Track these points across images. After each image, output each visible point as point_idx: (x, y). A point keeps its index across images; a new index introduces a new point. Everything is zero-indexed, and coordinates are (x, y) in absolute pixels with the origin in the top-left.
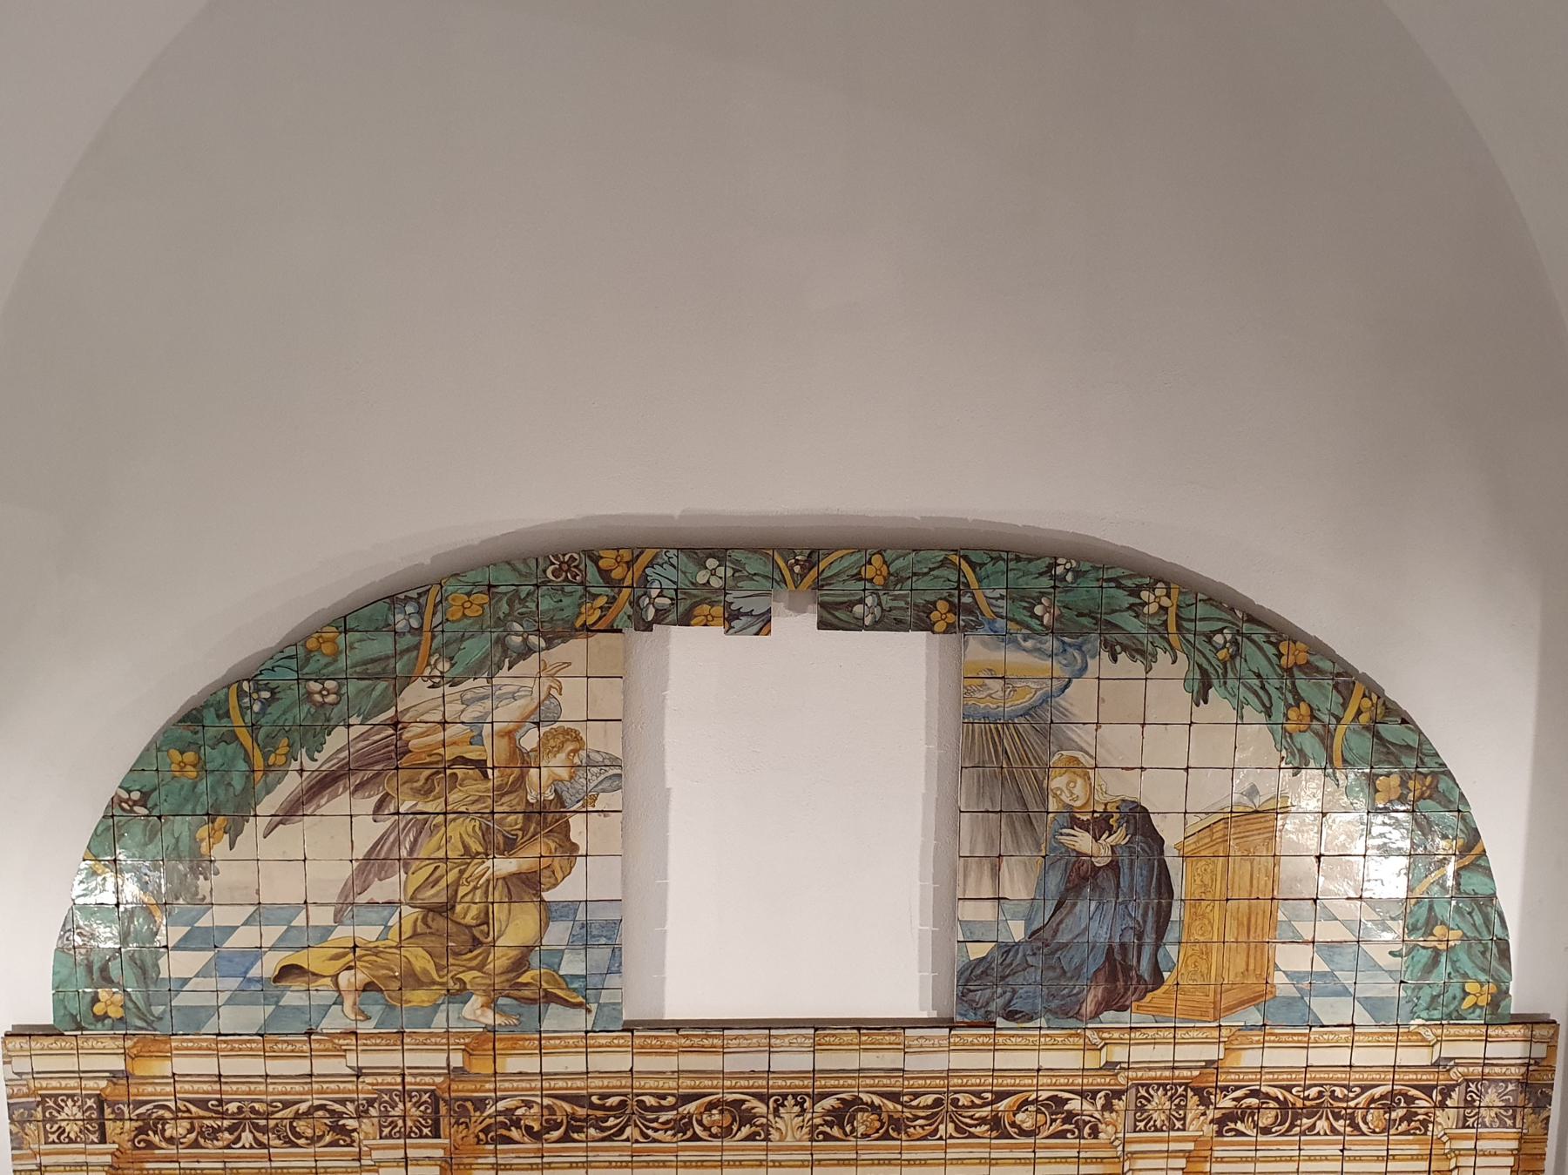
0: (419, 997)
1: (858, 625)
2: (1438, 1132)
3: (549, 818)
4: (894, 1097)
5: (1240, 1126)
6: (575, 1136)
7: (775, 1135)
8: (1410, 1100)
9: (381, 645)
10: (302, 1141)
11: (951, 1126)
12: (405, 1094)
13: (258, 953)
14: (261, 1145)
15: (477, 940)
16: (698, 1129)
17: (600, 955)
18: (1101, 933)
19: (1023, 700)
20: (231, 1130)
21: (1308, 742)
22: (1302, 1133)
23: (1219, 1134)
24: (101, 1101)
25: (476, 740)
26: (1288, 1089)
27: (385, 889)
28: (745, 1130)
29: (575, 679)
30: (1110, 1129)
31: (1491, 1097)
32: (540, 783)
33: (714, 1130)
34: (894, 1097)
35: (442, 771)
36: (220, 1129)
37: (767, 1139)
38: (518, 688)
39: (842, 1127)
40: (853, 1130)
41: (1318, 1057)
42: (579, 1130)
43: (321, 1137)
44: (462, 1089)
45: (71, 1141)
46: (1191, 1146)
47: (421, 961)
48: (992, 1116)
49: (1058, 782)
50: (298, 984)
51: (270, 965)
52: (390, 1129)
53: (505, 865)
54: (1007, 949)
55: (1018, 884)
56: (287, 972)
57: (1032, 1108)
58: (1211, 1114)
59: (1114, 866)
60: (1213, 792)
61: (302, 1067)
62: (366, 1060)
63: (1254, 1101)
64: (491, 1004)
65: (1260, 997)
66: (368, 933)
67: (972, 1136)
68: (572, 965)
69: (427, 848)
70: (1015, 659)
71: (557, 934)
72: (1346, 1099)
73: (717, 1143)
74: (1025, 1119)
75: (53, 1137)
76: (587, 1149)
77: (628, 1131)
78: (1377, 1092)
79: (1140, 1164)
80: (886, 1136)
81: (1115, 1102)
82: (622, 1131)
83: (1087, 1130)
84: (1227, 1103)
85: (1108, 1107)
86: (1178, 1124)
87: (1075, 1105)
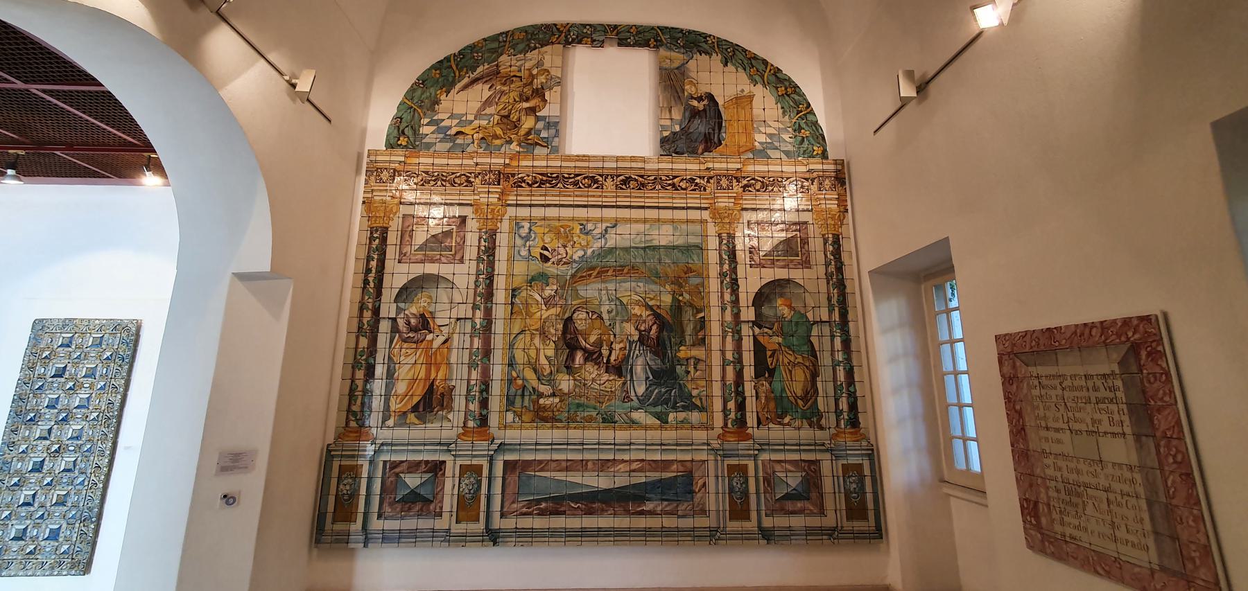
0: (497, 142)
1: (628, 45)
3: (539, 93)
4: (642, 176)
9: (495, 45)
12: (491, 171)
13: (450, 128)
15: (516, 126)
17: (553, 131)
18: (702, 129)
19: (676, 64)
21: (757, 78)
24: (395, 170)
25: (520, 71)
27: (490, 110)
29: (550, 56)
31: (827, 182)
32: (537, 83)
34: (642, 176)
35: (508, 80)
38: (533, 55)
41: (771, 168)
44: (508, 170)
47: (499, 132)
48: (671, 183)
49: (687, 87)
50: (461, 137)
51: (453, 131)
52: (484, 182)
53: (526, 105)
54: (674, 133)
55: (677, 114)
56: (458, 133)
59: (704, 110)
60: (731, 91)
61: (459, 162)
62: (479, 160)
64: (519, 145)
65: (752, 150)
66: (484, 123)
68: (544, 134)
69: (504, 99)
70: (674, 54)
71: (540, 125)
74: (683, 185)
84: (745, 182)
87: (698, 181)
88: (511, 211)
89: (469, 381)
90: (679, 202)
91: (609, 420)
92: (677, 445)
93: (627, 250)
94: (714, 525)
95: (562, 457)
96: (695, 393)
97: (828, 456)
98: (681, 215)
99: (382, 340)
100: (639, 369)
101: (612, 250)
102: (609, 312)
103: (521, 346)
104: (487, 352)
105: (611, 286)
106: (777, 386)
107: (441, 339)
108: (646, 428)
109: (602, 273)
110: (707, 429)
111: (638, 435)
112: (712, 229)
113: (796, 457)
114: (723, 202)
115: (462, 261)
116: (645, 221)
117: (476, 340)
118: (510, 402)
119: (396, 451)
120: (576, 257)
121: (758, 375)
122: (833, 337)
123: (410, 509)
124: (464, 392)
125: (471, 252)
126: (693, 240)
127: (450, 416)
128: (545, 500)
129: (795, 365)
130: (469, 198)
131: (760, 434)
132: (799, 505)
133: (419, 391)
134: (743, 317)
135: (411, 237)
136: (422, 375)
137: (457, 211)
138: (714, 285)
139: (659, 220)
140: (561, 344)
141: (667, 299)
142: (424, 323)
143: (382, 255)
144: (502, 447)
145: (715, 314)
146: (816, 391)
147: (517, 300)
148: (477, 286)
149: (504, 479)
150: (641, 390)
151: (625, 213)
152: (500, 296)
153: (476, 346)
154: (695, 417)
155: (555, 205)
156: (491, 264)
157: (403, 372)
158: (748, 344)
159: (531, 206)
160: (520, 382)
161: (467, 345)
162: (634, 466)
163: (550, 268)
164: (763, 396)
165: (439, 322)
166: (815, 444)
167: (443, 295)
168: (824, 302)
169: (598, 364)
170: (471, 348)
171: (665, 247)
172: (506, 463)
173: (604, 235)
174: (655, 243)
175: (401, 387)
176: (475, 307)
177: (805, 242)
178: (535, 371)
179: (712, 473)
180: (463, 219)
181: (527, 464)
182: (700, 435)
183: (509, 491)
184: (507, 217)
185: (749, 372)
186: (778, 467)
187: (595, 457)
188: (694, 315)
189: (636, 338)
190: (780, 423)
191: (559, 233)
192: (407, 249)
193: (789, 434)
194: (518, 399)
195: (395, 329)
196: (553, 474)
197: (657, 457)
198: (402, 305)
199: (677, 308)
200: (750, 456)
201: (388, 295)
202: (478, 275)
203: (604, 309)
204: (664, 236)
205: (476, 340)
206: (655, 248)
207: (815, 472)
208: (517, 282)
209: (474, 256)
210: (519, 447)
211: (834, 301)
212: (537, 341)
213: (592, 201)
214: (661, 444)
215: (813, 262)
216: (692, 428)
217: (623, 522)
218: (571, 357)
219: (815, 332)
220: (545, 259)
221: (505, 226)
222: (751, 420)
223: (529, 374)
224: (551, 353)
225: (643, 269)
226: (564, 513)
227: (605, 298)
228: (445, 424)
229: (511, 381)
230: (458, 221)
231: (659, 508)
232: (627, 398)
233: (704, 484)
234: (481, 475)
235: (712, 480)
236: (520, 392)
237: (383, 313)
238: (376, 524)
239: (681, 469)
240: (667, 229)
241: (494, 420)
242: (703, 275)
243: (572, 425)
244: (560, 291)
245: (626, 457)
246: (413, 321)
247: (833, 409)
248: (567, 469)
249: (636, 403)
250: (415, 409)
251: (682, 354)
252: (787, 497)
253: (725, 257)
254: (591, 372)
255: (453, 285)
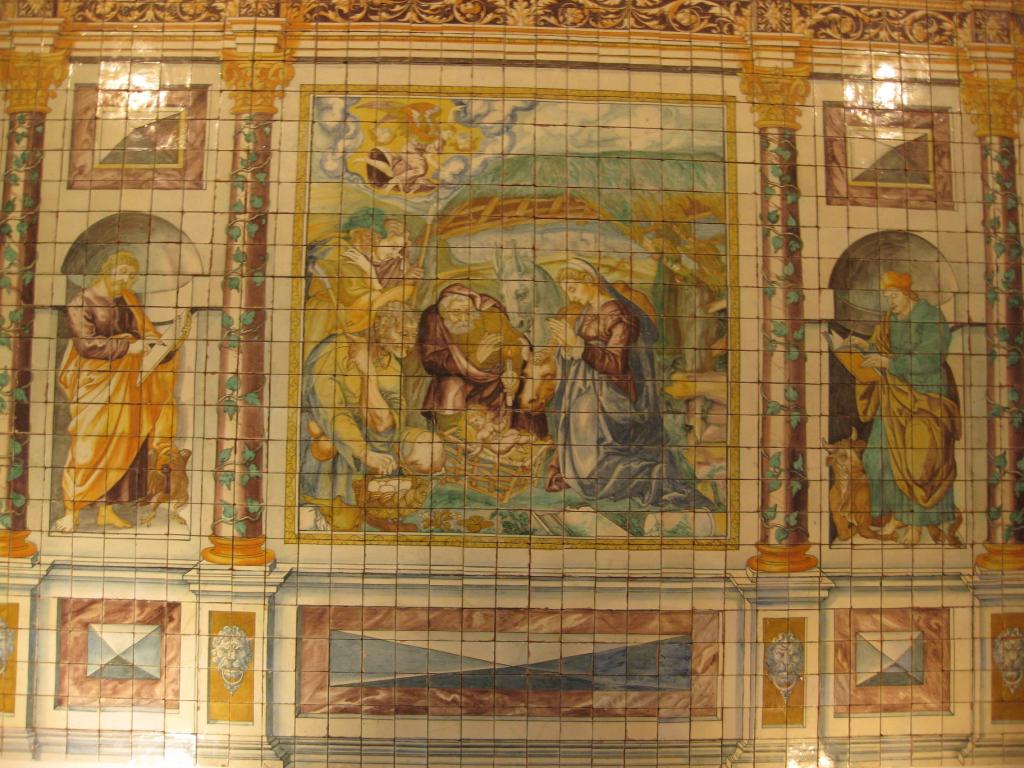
2: (960, 44)
5: (829, 31)
6: (372, 17)
7: (510, 21)
8: (940, 22)
10: (186, 18)
11: (632, 20)
14: (158, 19)
16: (457, 15)
20: (140, 9)
22: (871, 39)
23: (816, 36)
26: (858, 8)
28: (490, 17)
30: (741, 28)
33: (468, 16)
36: (132, 9)
37: (505, 24)
39: (556, 16)
40: (565, 20)
42: (375, 13)
43: (199, 15)
45: (34, 16)
46: (796, 44)
57: (687, 11)
58: (809, 22)
63: (835, 16)
67: (647, 28)
72: (897, 18)
73: (469, 25)
74: (684, 18)
75: (23, 12)
76: (380, 27)
77: (409, 16)
78: (918, 14)
79: (764, 54)
80: (587, 25)
81: (743, 10)
82: (404, 15)
83: (725, 28)
84: (818, 16)
85: (738, 13)
86: (787, 28)
87: (716, 10)
88: (304, 74)
89: (219, 440)
90: (674, 57)
91: (518, 529)
92: (662, 579)
93: (559, 159)
94: (731, 733)
95: (418, 601)
96: (702, 472)
97: (965, 599)
98: (678, 84)
99: (41, 354)
100: (583, 421)
101: (525, 160)
102: (519, 296)
103: (329, 368)
104: (256, 381)
105: (524, 240)
106: (873, 458)
107: (159, 353)
108: (597, 544)
109: (503, 212)
110: (726, 547)
111: (579, 559)
112: (746, 118)
113: (902, 601)
114: (770, 60)
115: (198, 184)
116: (599, 96)
117: (232, 355)
118: (306, 489)
119: (80, 580)
120: (446, 174)
121: (836, 437)
122: (991, 355)
123: (115, 691)
124: (211, 464)
125: (218, 165)
126: (705, 142)
127: (184, 513)
128: (386, 685)
129: (912, 415)
130: (213, 46)
131: (834, 557)
132: (902, 694)
133: (119, 462)
134: (809, 312)
135: (92, 131)
136: (124, 426)
137: (188, 76)
138: (748, 240)
139: (628, 95)
140: (414, 365)
141: (646, 269)
142: (124, 318)
143: (36, 168)
144: (293, 579)
145: (749, 303)
146: (953, 468)
147: (318, 270)
148: (231, 239)
149: (297, 640)
150: (587, 464)
151: (555, 79)
152: (281, 260)
153: (232, 367)
154: (703, 523)
155: (401, 60)
156: (262, 191)
157: (86, 421)
158: (817, 369)
159: (346, 61)
160: (327, 445)
161: (214, 366)
162: (571, 621)
163: (389, 199)
164: (844, 478)
165: (154, 315)
166: (944, 576)
167: (160, 258)
168: (978, 280)
169: (495, 408)
170: (222, 373)
171: (646, 157)
172: (303, 611)
173: (507, 126)
174: (622, 145)
175: (84, 451)
176: (228, 284)
177: (942, 151)
178: (359, 421)
179: (732, 635)
180: (201, 93)
181: (346, 615)
182: (711, 560)
183: (314, 662)
184: (294, 85)
185: (817, 430)
186: (865, 623)
187: (489, 603)
188: (705, 306)
189: (578, 353)
190: (875, 535)
191: (409, 121)
192: (84, 159)
193: (895, 557)
194: (324, 483)
195: (65, 331)
196: (402, 635)
197: (619, 604)
198: (77, 279)
199: (670, 288)
200: (809, 601)
201: (50, 257)
202: (233, 214)
203: (509, 291)
204: (640, 130)
205: (232, 355)
206: (619, 156)
207: (938, 630)
208: (320, 228)
209: (225, 172)
210: (328, 579)
211: (999, 279)
212: (362, 357)
213: (482, 50)
214: (629, 579)
215: (957, 195)
216: (695, 544)
217: (544, 729)
218: (437, 393)
219: (957, 343)
220: (380, 179)
221: (290, 105)
222: (817, 529)
223: (347, 430)
224: (392, 383)
225: (592, 200)
226: (425, 710)
227: (509, 265)
228: (175, 528)
229: (308, 443)
230: (191, 96)
231: (620, 704)
232: (556, 483)
233: (715, 658)
234: (251, 633)
235: (731, 649)
236: (327, 466)
237: (39, 298)
238: (51, 718)
239: (668, 627)
240: (648, 115)
241: (274, 524)
242: (722, 213)
243: (439, 536)
244: (412, 250)
245: (555, 604)
246: (101, 314)
247: (982, 505)
248: (429, 626)
249: (575, 493)
250: (113, 495)
251: (676, 390)
252: (882, 680)
253: (773, 179)
254: (480, 424)
255: (180, 238)
